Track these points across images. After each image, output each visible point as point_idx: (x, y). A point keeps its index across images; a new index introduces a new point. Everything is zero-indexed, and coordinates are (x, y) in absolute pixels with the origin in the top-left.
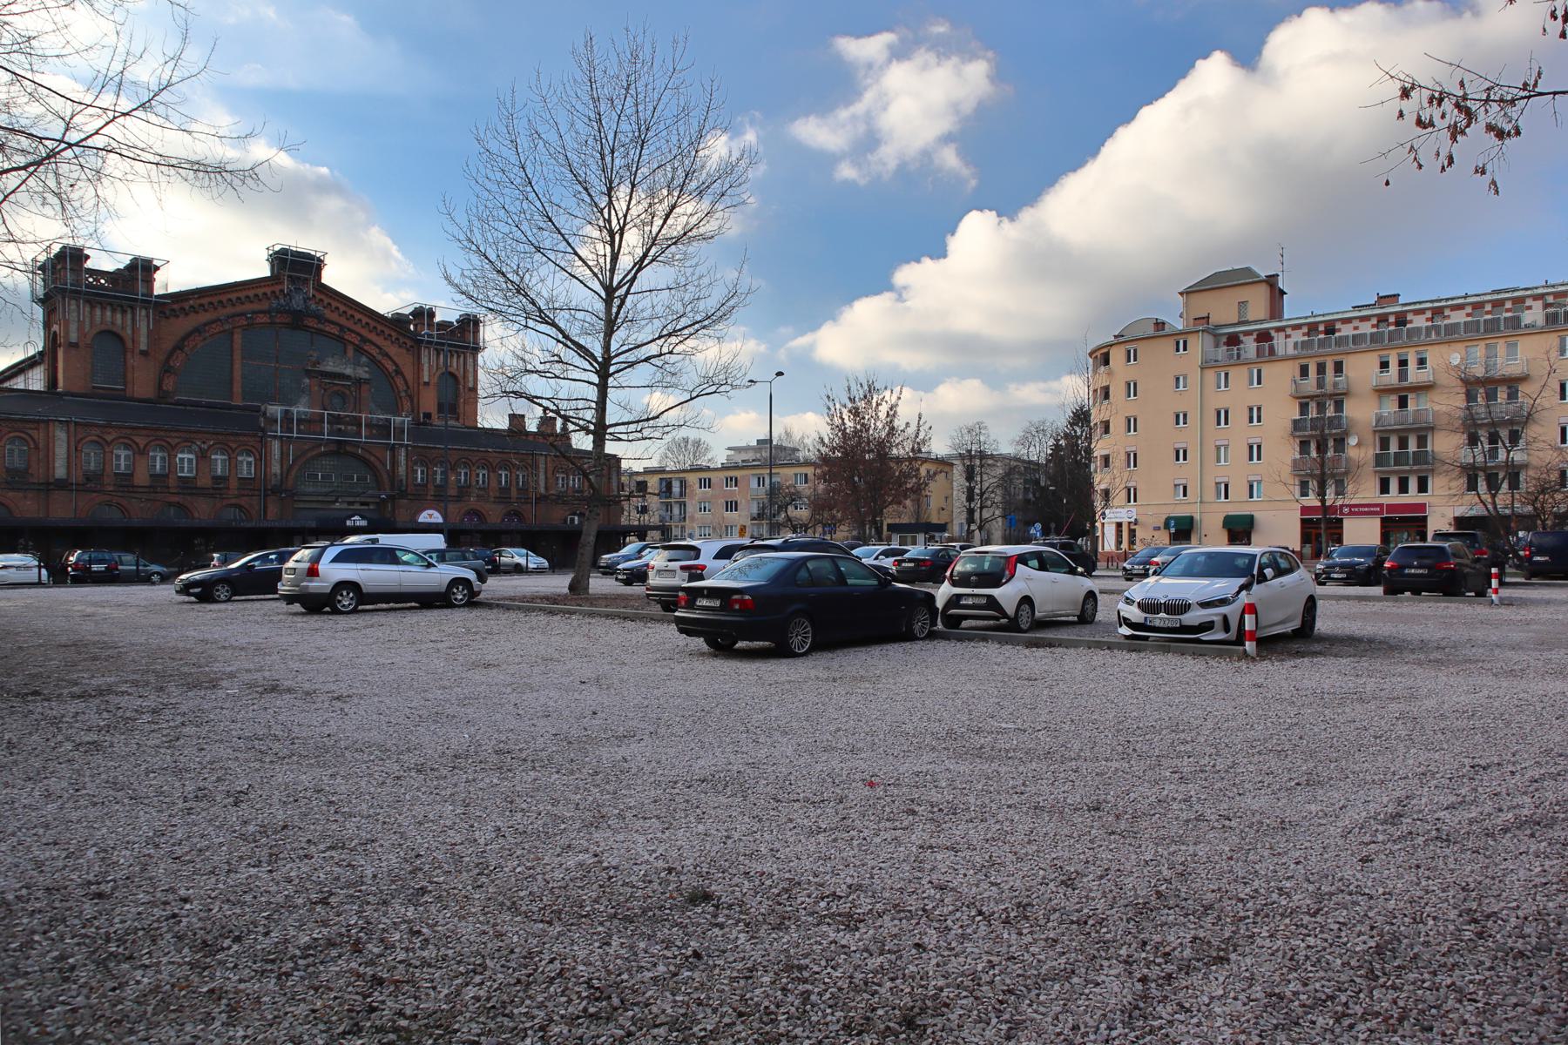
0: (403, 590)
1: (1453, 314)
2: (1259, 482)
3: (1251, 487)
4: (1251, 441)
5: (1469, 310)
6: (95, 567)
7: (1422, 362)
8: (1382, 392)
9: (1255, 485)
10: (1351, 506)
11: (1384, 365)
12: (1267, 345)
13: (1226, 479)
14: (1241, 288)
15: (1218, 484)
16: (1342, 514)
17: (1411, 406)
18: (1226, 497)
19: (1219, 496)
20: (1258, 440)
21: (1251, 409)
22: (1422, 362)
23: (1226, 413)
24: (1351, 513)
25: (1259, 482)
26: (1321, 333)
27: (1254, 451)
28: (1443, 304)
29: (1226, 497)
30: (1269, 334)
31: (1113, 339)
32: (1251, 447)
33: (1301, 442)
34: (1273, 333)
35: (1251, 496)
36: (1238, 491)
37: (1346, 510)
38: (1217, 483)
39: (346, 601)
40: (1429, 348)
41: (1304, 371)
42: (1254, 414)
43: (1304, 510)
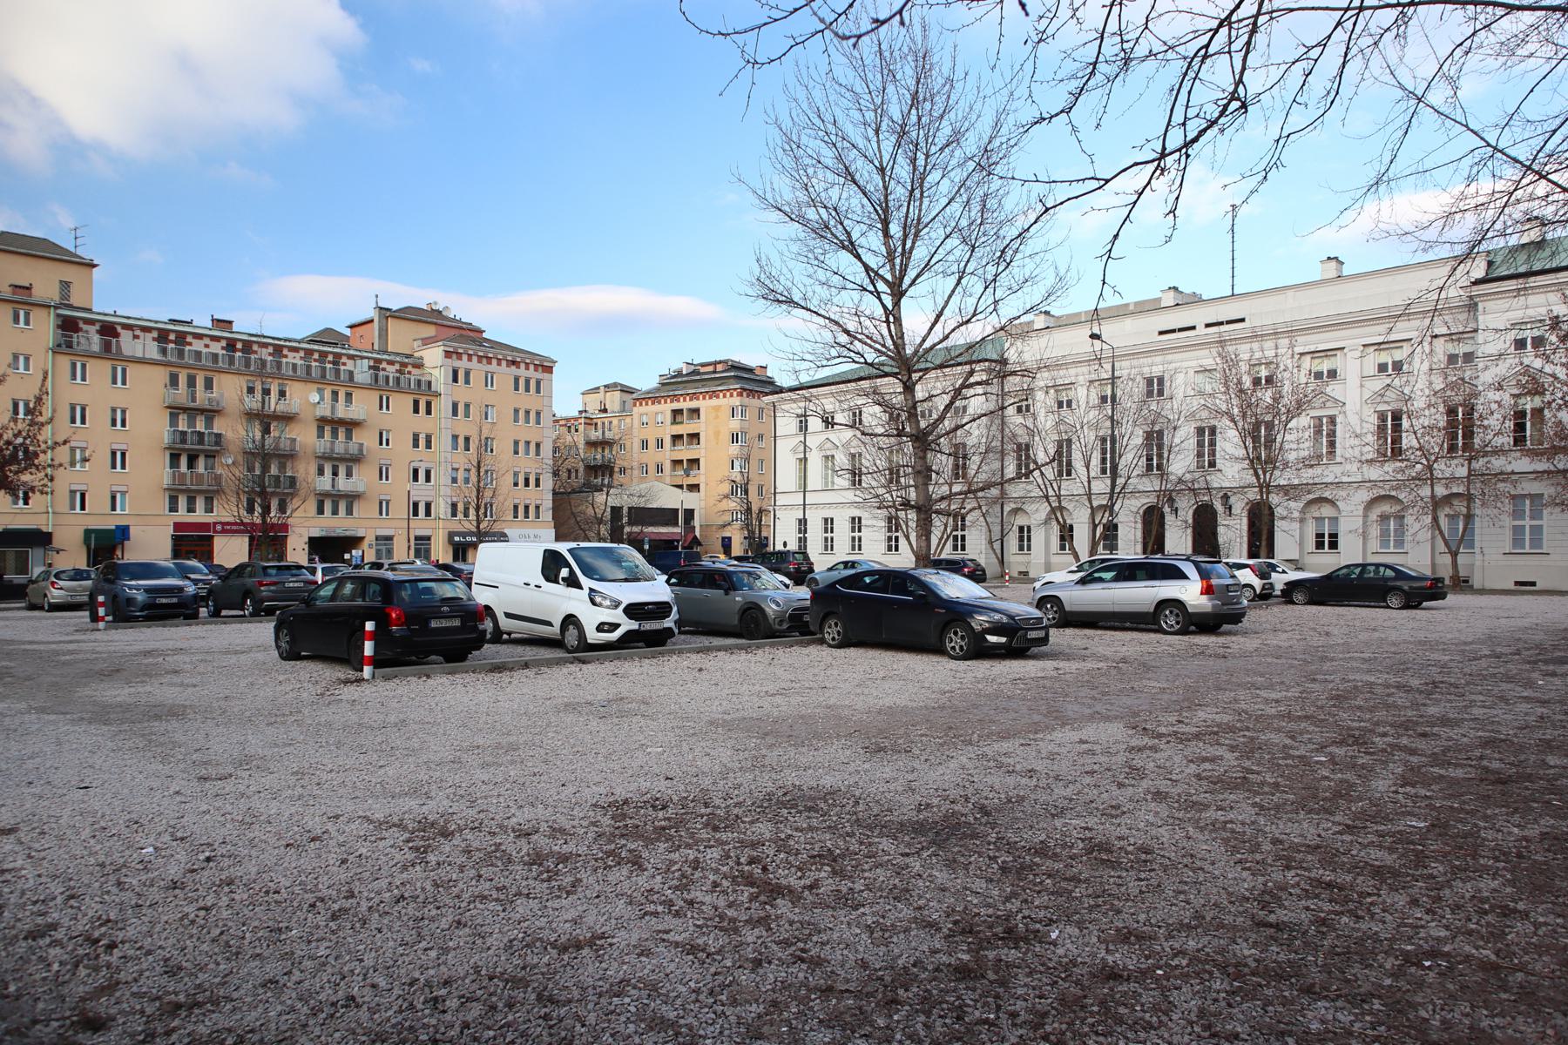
0: (1117, 609)
1: (291, 355)
2: (123, 493)
3: (114, 498)
4: (114, 447)
5: (302, 354)
6: (992, 639)
7: (282, 394)
8: (250, 416)
9: (118, 496)
10: (223, 524)
11: (251, 390)
12: (114, 340)
13: (83, 488)
14: (22, 260)
15: (73, 492)
16: (215, 532)
17: (274, 433)
18: (83, 508)
19: (73, 507)
20: (123, 447)
21: (114, 410)
22: (282, 394)
23: (83, 410)
24: (224, 531)
25: (123, 493)
26: (171, 341)
27: (118, 458)
28: (282, 343)
29: (83, 508)
30: (77, 324)
31: (209, 325)
32: (114, 454)
33: (171, 455)
34: (119, 329)
35: (114, 509)
36: (98, 502)
37: (219, 527)
38: (71, 491)
39: (1170, 620)
40: (289, 382)
41: (174, 381)
42: (118, 418)
43: (177, 526)
